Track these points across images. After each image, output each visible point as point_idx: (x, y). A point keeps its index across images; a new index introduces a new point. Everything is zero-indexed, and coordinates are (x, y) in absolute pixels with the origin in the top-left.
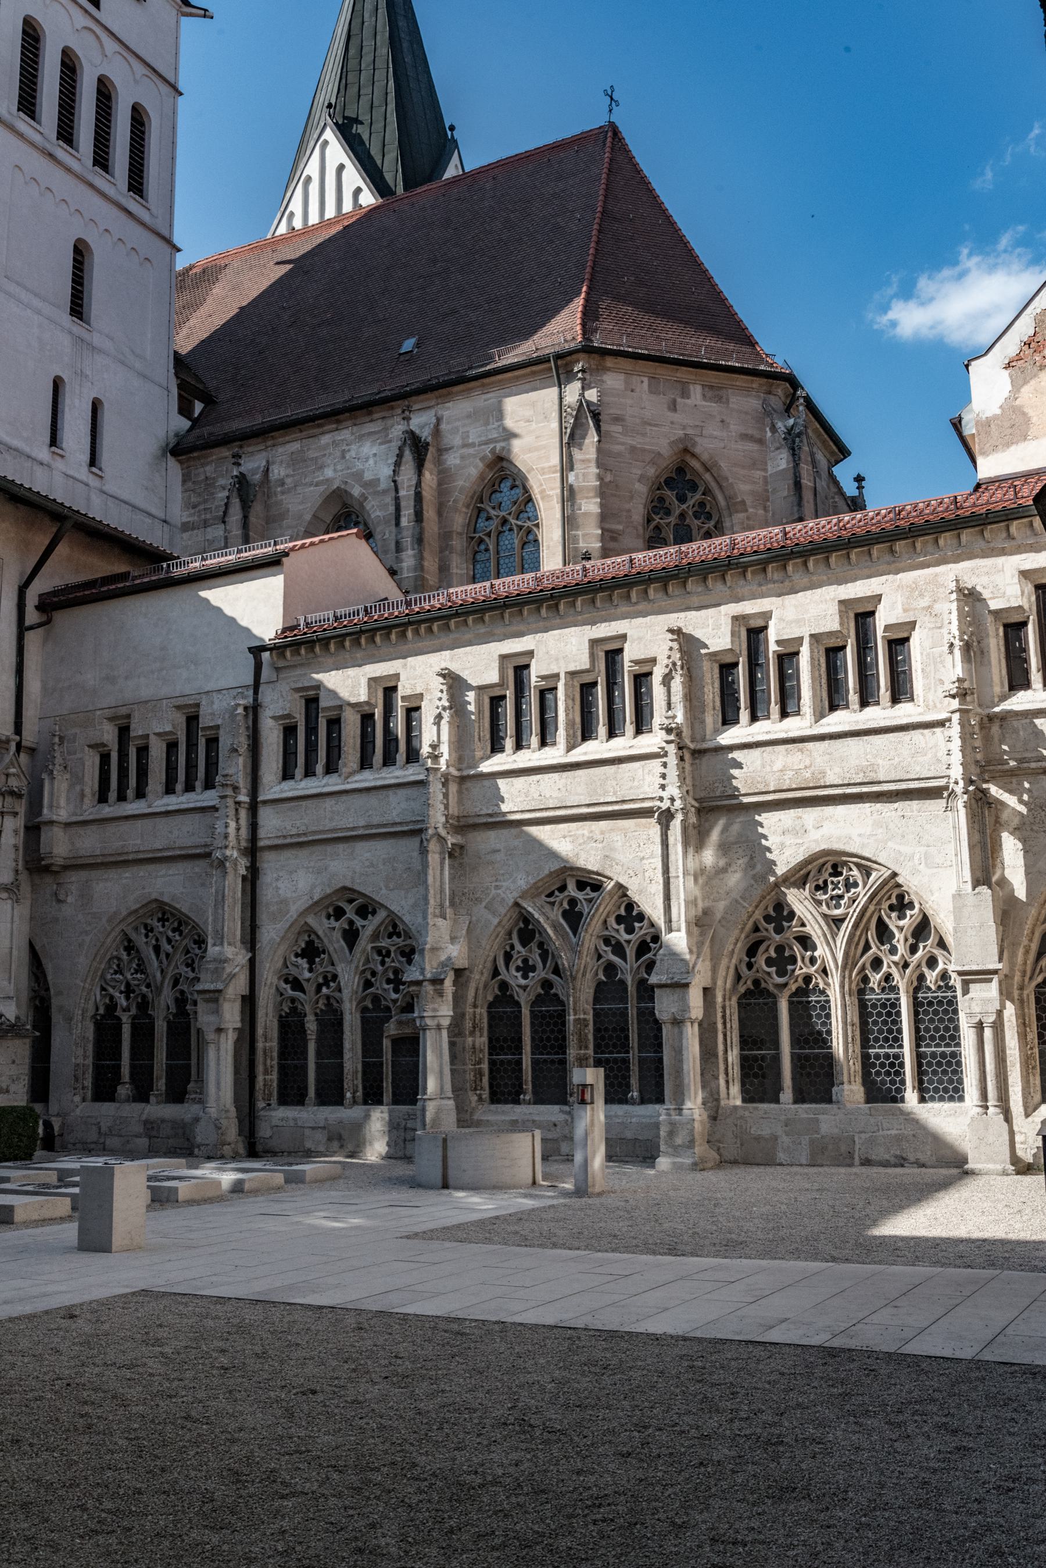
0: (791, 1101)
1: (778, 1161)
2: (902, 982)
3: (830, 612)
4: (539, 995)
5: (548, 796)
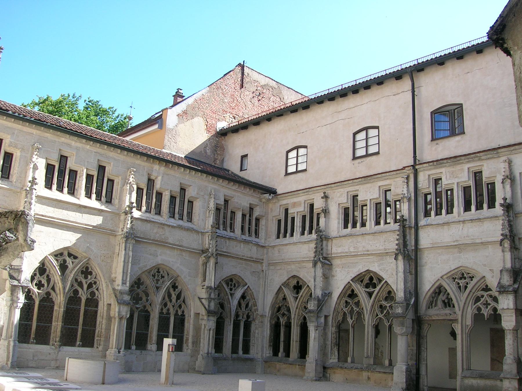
0: (135, 349)
1: (133, 370)
2: (172, 312)
3: (177, 185)
4: (44, 298)
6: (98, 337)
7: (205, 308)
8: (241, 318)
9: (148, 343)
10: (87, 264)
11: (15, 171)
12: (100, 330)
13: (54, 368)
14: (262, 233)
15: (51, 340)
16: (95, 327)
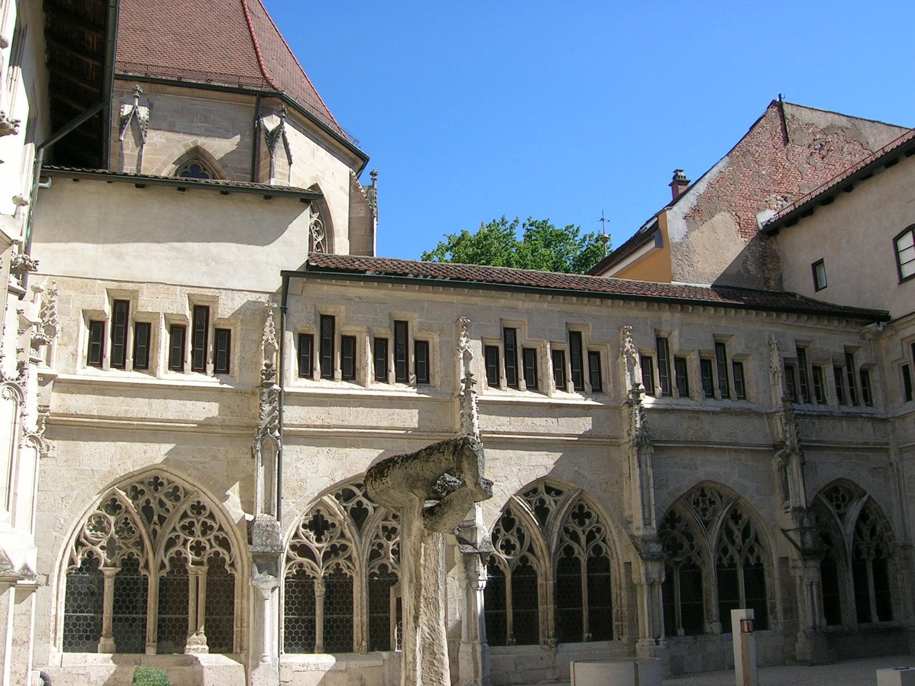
4: (518, 567)
5: (538, 424)
6: (617, 620)
7: (796, 546)
8: (865, 556)
9: (706, 620)
10: (579, 500)
11: (437, 369)
12: (619, 609)
13: (553, 681)
14: (877, 396)
15: (540, 636)
16: (611, 605)
